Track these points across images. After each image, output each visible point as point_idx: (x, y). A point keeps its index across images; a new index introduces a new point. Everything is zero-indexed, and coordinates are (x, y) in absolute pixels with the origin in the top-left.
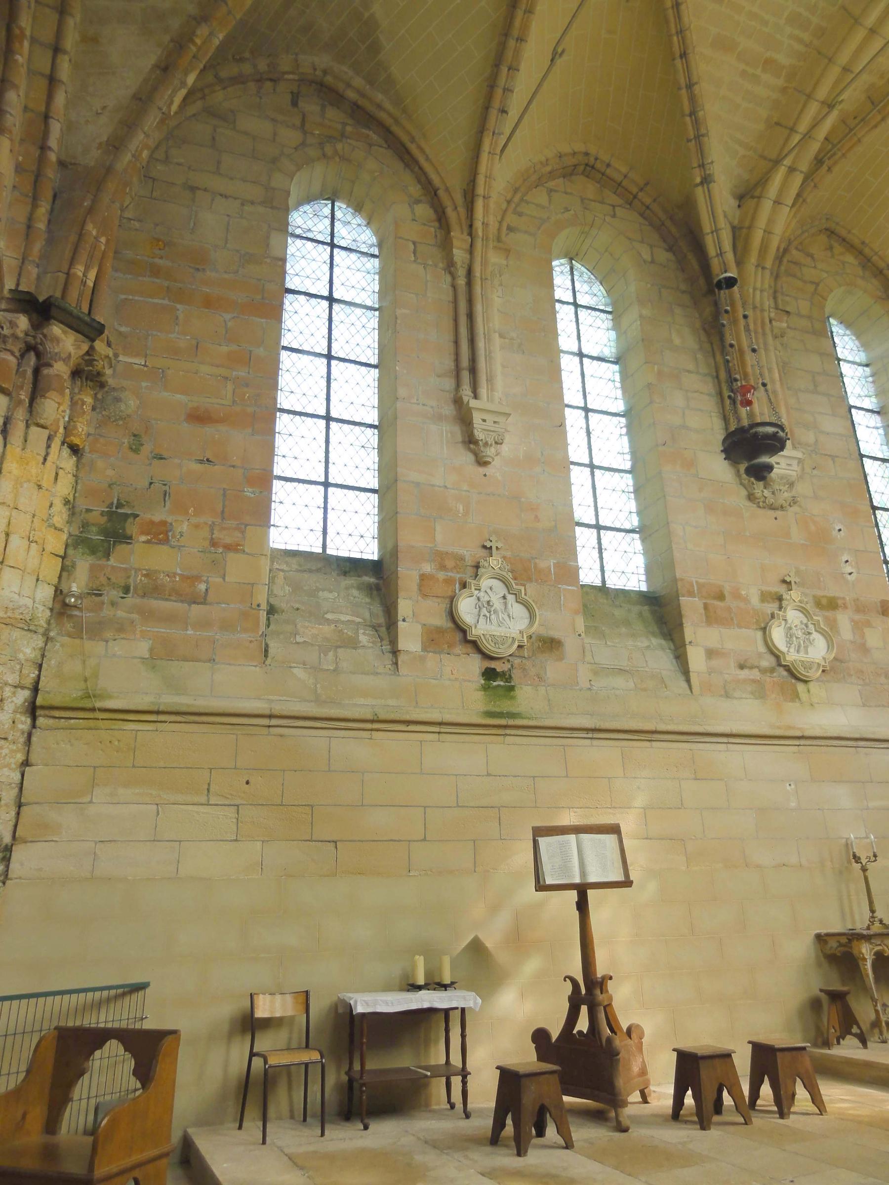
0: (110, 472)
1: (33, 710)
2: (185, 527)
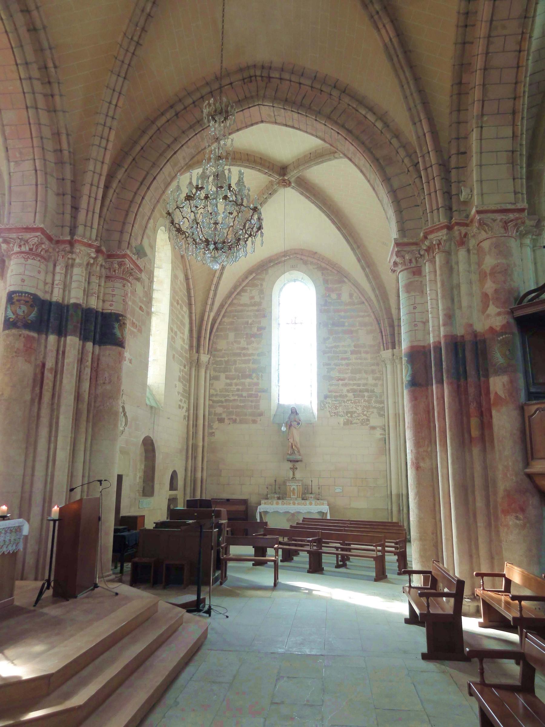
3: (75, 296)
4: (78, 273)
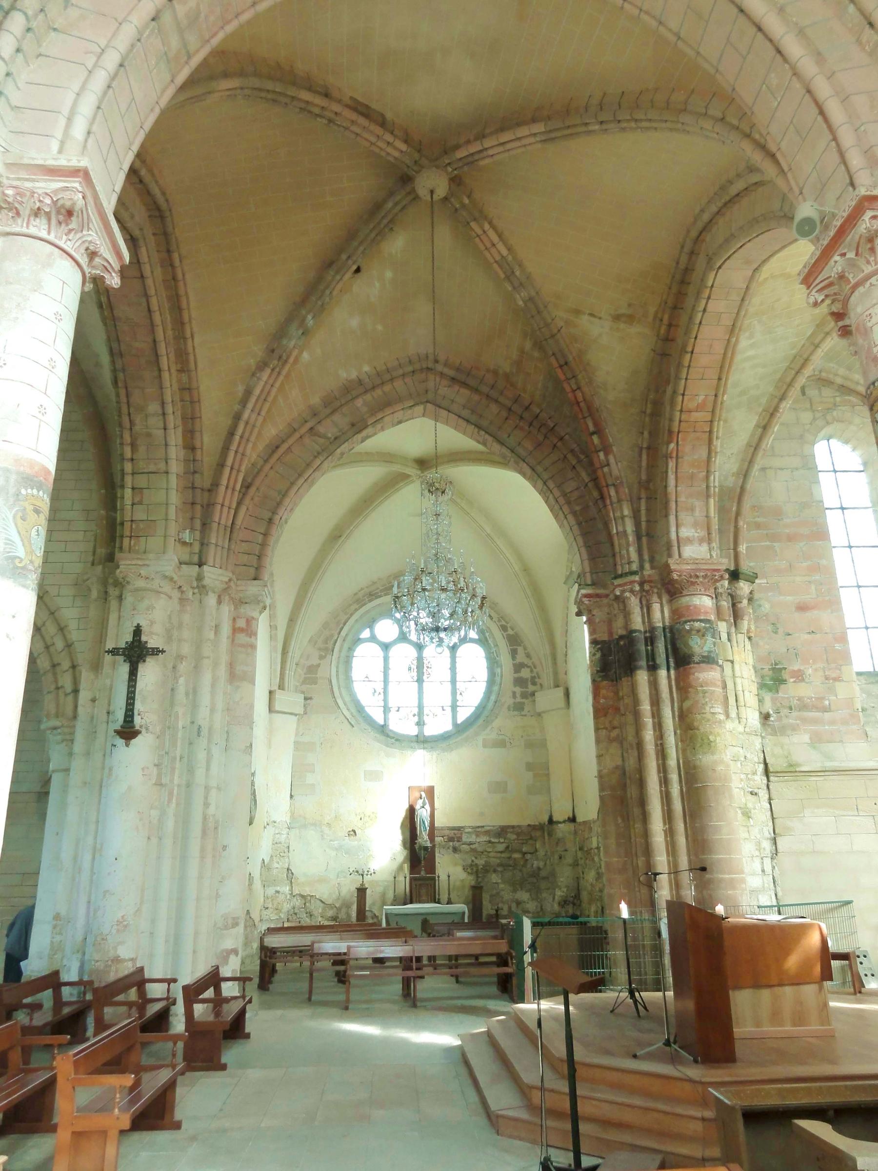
0: (767, 647)
1: (767, 772)
2: (810, 671)
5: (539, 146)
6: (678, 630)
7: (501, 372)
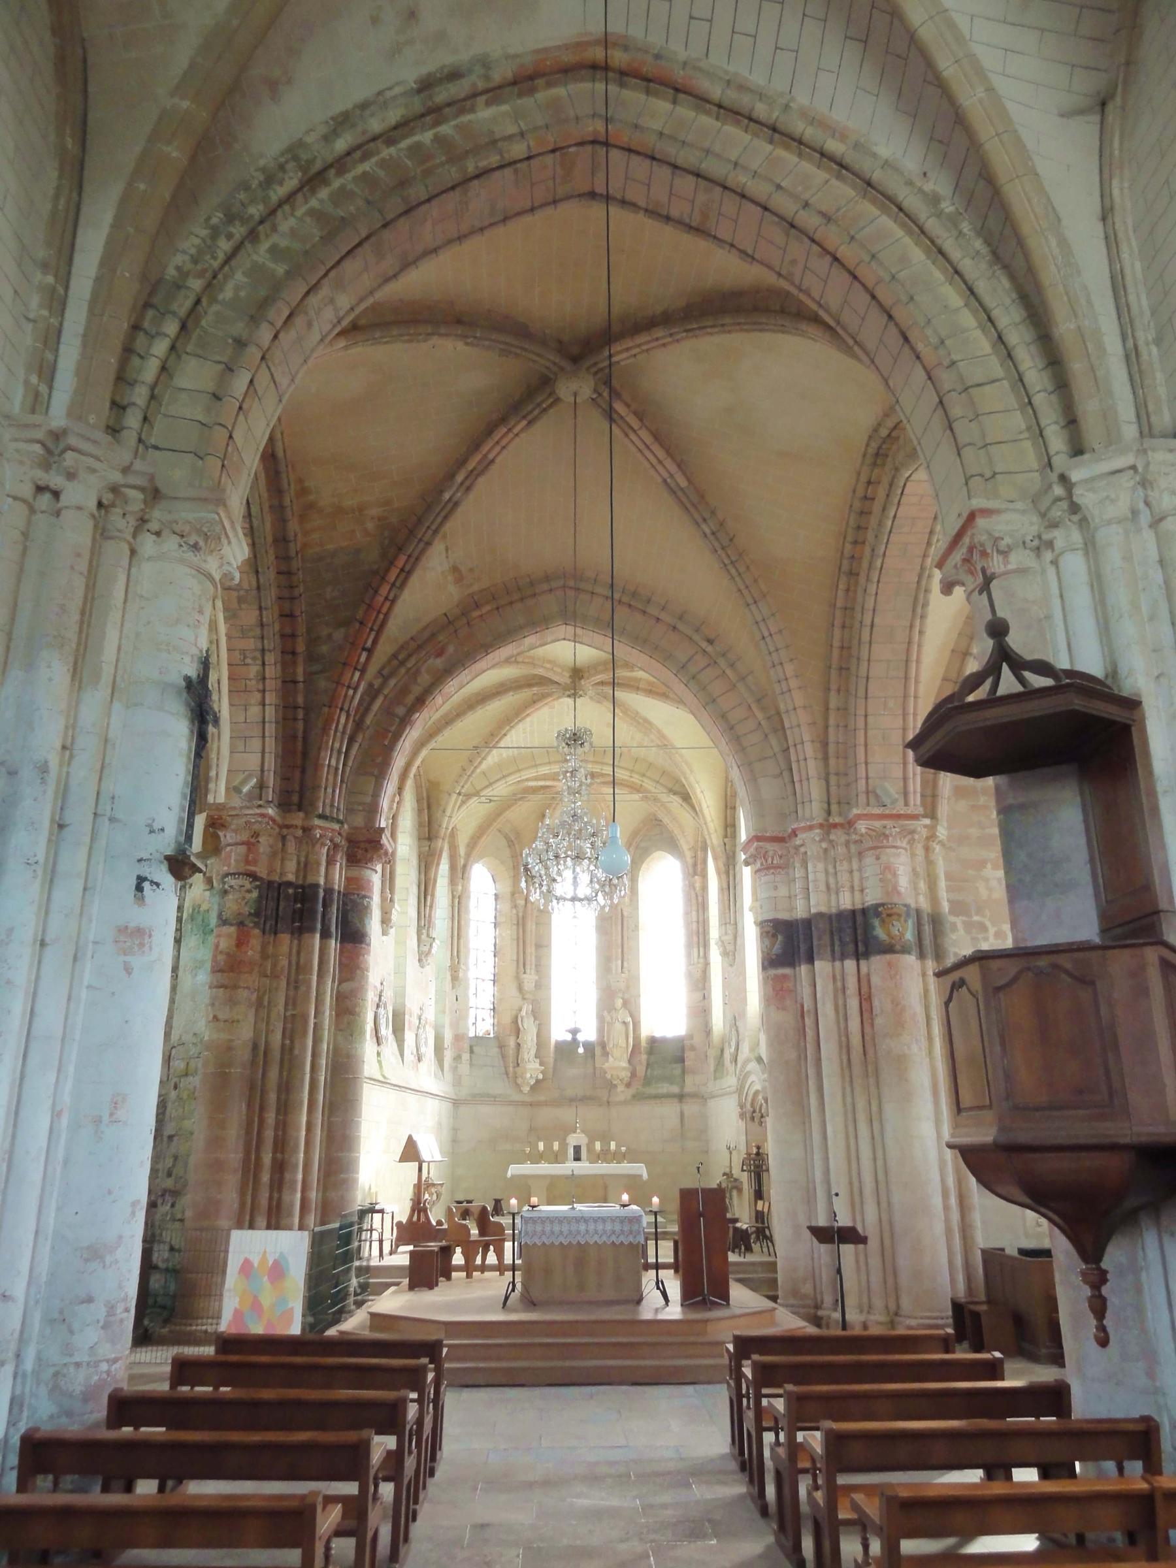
3: (819, 903)
4: (816, 870)
5: (660, 480)
6: (353, 901)
7: (311, 497)
